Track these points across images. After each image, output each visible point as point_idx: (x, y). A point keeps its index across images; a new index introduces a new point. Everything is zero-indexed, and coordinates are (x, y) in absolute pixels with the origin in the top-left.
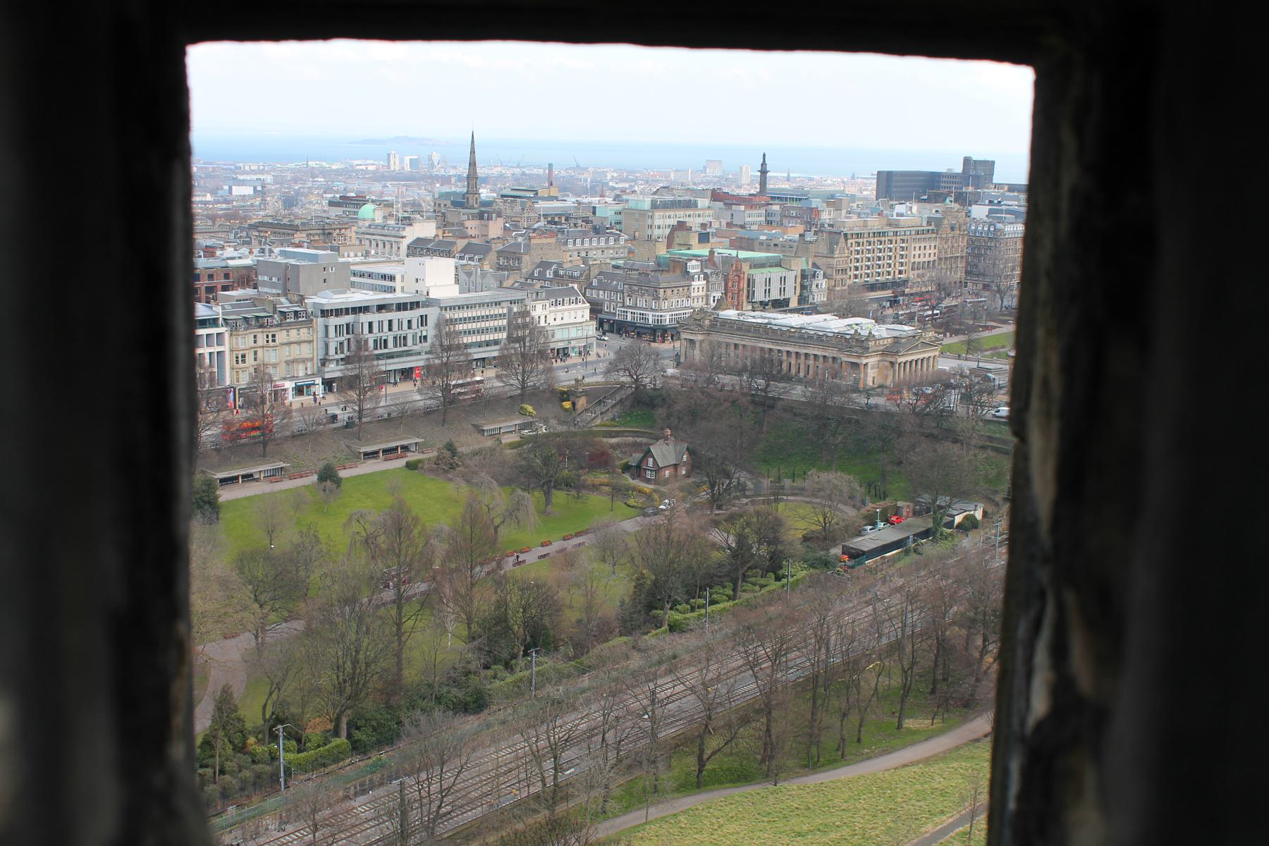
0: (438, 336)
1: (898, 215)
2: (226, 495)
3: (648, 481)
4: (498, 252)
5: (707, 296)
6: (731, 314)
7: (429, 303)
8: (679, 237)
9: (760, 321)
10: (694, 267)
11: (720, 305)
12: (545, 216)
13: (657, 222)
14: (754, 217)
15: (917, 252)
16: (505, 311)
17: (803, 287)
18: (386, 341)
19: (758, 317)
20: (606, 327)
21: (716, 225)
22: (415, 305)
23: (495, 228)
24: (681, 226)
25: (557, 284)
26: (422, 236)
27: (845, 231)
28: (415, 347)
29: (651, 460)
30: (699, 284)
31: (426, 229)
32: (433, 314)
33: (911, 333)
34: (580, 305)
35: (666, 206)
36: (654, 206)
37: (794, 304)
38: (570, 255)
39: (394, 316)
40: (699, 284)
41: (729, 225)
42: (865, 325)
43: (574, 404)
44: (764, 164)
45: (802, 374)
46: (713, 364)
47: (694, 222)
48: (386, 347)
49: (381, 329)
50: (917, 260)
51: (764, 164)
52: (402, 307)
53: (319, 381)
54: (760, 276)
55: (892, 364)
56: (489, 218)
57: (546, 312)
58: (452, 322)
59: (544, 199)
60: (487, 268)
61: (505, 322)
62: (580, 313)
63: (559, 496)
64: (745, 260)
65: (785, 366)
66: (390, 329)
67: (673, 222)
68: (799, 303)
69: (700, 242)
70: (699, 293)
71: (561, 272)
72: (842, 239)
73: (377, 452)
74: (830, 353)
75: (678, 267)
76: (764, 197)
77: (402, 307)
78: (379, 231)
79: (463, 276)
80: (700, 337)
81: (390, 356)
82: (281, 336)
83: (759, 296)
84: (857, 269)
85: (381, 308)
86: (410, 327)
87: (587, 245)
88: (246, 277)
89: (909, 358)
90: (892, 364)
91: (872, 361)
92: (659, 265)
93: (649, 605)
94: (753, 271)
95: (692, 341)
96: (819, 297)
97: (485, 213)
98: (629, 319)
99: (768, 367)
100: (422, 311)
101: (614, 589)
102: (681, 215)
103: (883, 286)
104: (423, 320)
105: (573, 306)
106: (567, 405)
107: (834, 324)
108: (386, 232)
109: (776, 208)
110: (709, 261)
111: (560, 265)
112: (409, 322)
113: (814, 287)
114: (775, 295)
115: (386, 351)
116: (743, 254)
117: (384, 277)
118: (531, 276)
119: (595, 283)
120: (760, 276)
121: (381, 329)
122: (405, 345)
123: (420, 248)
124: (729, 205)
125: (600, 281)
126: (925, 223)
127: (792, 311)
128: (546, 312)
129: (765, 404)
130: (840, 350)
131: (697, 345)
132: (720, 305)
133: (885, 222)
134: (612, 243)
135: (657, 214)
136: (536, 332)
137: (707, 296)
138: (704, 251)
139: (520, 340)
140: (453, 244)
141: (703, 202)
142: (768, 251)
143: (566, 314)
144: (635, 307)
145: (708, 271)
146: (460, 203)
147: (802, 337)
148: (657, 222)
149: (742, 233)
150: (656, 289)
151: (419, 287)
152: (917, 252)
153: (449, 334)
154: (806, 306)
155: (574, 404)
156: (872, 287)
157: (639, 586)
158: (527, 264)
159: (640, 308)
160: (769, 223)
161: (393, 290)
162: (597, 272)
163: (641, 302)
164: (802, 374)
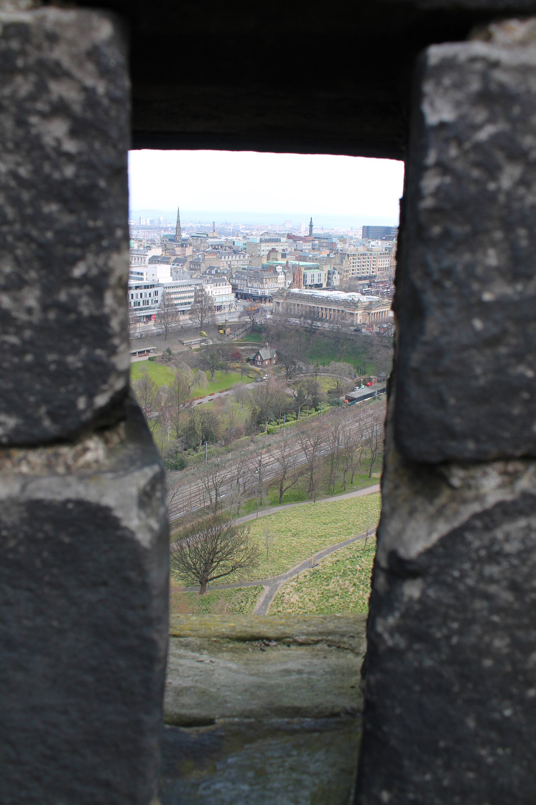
0: (163, 300)
1: (372, 246)
3: (258, 366)
4: (190, 262)
5: (285, 282)
6: (296, 290)
7: (159, 285)
8: (272, 255)
9: (309, 294)
10: (279, 269)
11: (291, 286)
12: (212, 246)
13: (262, 248)
14: (306, 247)
15: (380, 263)
16: (193, 289)
17: (329, 278)
18: (139, 303)
20: (239, 296)
21: (289, 250)
22: (152, 286)
23: (189, 251)
24: (273, 250)
25: (217, 276)
27: (348, 253)
28: (152, 305)
29: (259, 357)
30: (281, 277)
31: (157, 252)
32: (160, 290)
33: (377, 300)
34: (227, 286)
35: (267, 241)
36: (261, 241)
37: (324, 286)
38: (223, 263)
39: (143, 291)
40: (281, 277)
41: (295, 250)
42: (356, 296)
43: (224, 331)
44: (311, 222)
45: (328, 318)
46: (288, 313)
47: (279, 248)
48: (139, 305)
49: (137, 297)
50: (380, 266)
51: (311, 222)
52: (146, 287)
55: (369, 313)
57: (212, 289)
58: (169, 294)
59: (211, 238)
60: (185, 269)
61: (193, 294)
62: (227, 290)
63: (218, 373)
64: (303, 266)
65: (320, 314)
66: (141, 297)
67: (270, 248)
68: (327, 286)
69: (282, 257)
70: (281, 281)
71: (219, 271)
72: (347, 257)
73: (135, 353)
74: (341, 308)
75: (272, 269)
76: (311, 237)
77: (146, 287)
78: (136, 253)
79: (174, 273)
80: (282, 301)
81: (141, 309)
83: (309, 283)
84: (353, 270)
86: (150, 296)
87: (230, 259)
89: (377, 311)
90: (369, 313)
91: (360, 312)
92: (263, 268)
93: (258, 422)
94: (306, 271)
95: (278, 303)
96: (336, 282)
97: (184, 244)
98: (250, 293)
99: (312, 315)
100: (155, 289)
101: (243, 415)
102: (273, 245)
103: (365, 278)
104: (156, 293)
105: (224, 286)
106: (221, 331)
107: (343, 296)
108: (139, 253)
109: (317, 242)
110: (286, 266)
111: (218, 268)
112: (150, 294)
113: (334, 278)
114: (316, 282)
115: (139, 307)
116: (302, 263)
117: (138, 273)
118: (205, 273)
119: (234, 276)
120: (309, 273)
121: (137, 297)
122: (148, 304)
123: (154, 260)
124: (295, 241)
125: (236, 275)
126: (384, 250)
127: (324, 289)
128: (212, 289)
129: (312, 331)
130: (345, 307)
131: (281, 304)
132: (291, 286)
133: (366, 249)
134: (242, 258)
135: (263, 245)
136: (207, 298)
137: (285, 282)
138: (284, 262)
139: (200, 302)
141: (283, 239)
142: (313, 262)
143: (221, 290)
144: (252, 287)
145: (286, 271)
146: (173, 239)
147: (328, 301)
148: (262, 248)
149: (301, 253)
150: (262, 279)
151: (154, 278)
152: (380, 263)
153: (168, 299)
154: (330, 287)
155: (224, 331)
156: (360, 279)
157: (254, 413)
158: (204, 267)
159: (254, 288)
160: (313, 249)
161: (142, 279)
162: (235, 271)
163: (255, 285)
164: (328, 318)
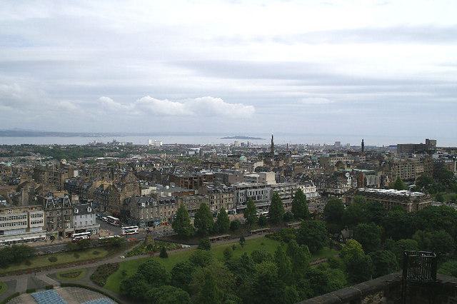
2: (212, 245)
6: (362, 189)
7: (268, 186)
10: (347, 175)
19: (371, 190)
23: (281, 163)
25: (305, 181)
31: (261, 164)
38: (308, 171)
53: (235, 210)
54: (368, 178)
75: (343, 175)
82: (225, 196)
88: (210, 178)
100: (266, 189)
116: (363, 171)
120: (368, 178)
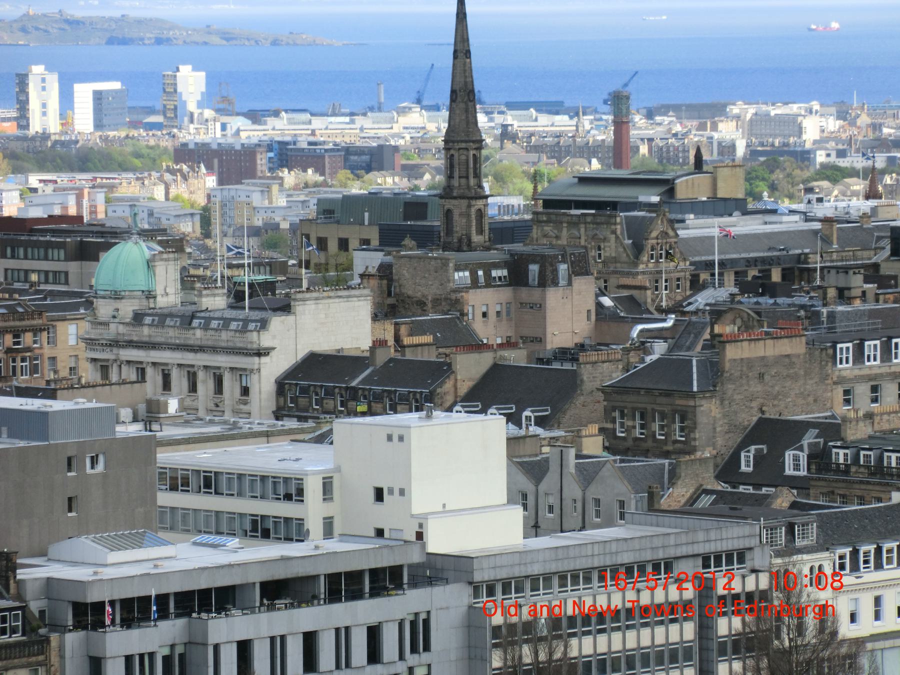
7: (434, 571)
22: (385, 580)
23: (568, 313)
26: (325, 344)
31: (338, 323)
52: (344, 586)
56: (547, 280)
61: (689, 630)
71: (841, 456)
77: (344, 586)
78: (172, 334)
85: (278, 591)
87: (873, 364)
108: (197, 335)
111: (831, 430)
112: (374, 634)
123: (320, 390)
140: (443, 370)
151: (386, 515)
161: (293, 530)
